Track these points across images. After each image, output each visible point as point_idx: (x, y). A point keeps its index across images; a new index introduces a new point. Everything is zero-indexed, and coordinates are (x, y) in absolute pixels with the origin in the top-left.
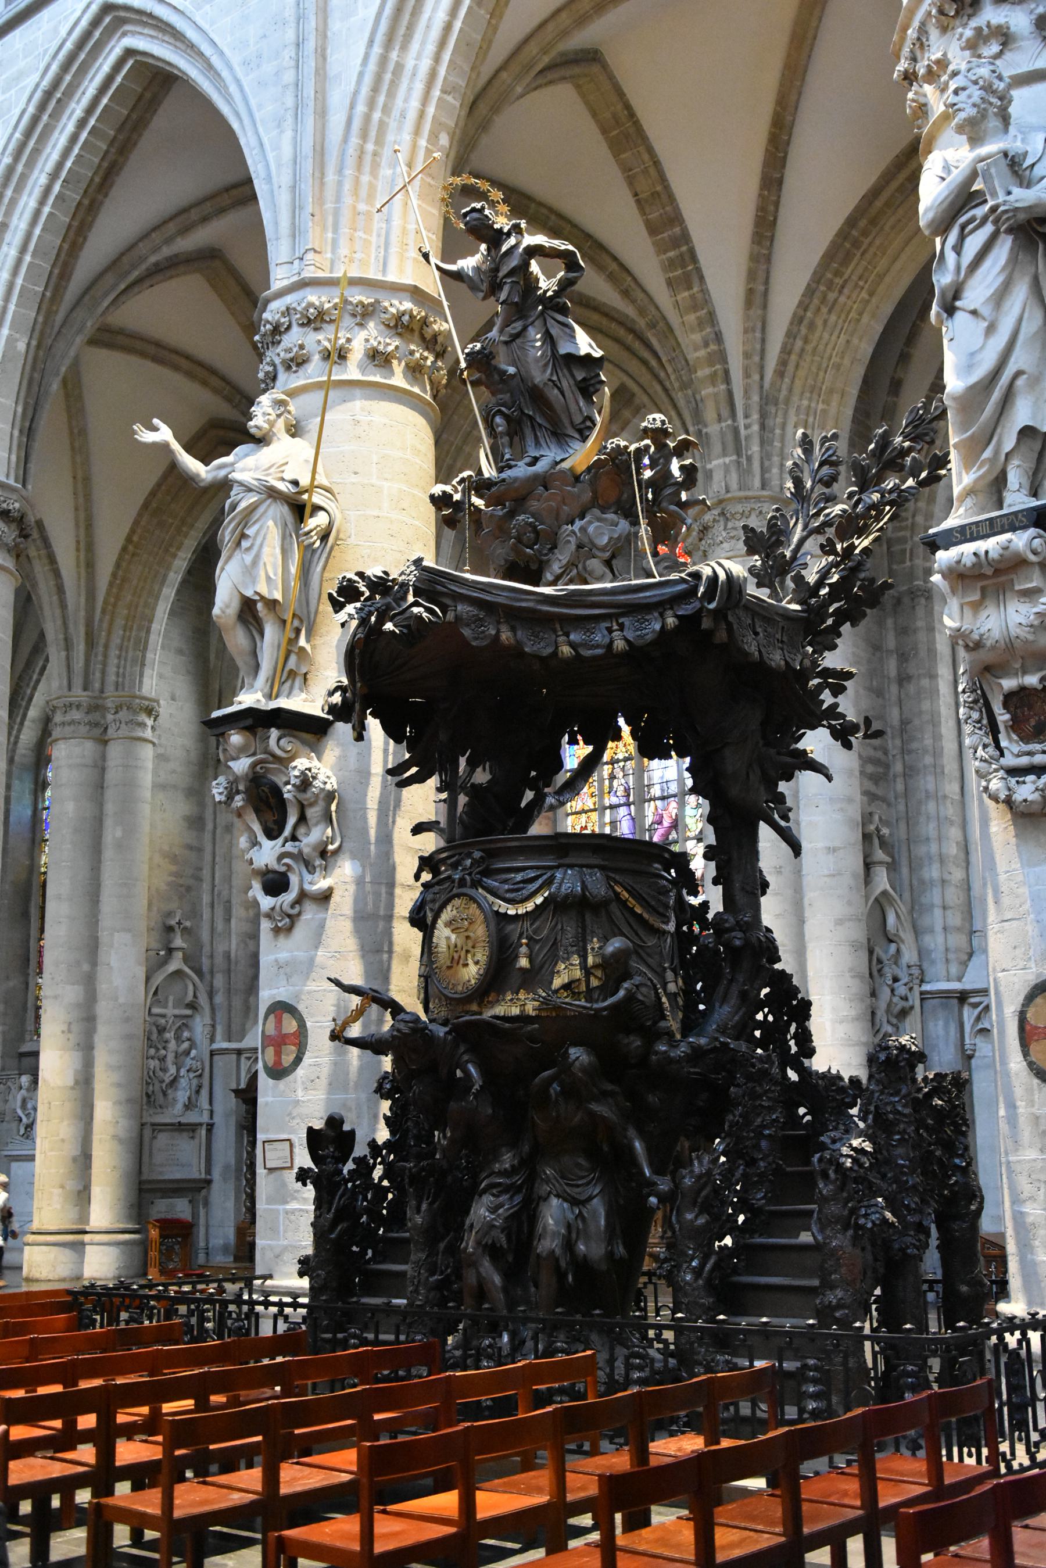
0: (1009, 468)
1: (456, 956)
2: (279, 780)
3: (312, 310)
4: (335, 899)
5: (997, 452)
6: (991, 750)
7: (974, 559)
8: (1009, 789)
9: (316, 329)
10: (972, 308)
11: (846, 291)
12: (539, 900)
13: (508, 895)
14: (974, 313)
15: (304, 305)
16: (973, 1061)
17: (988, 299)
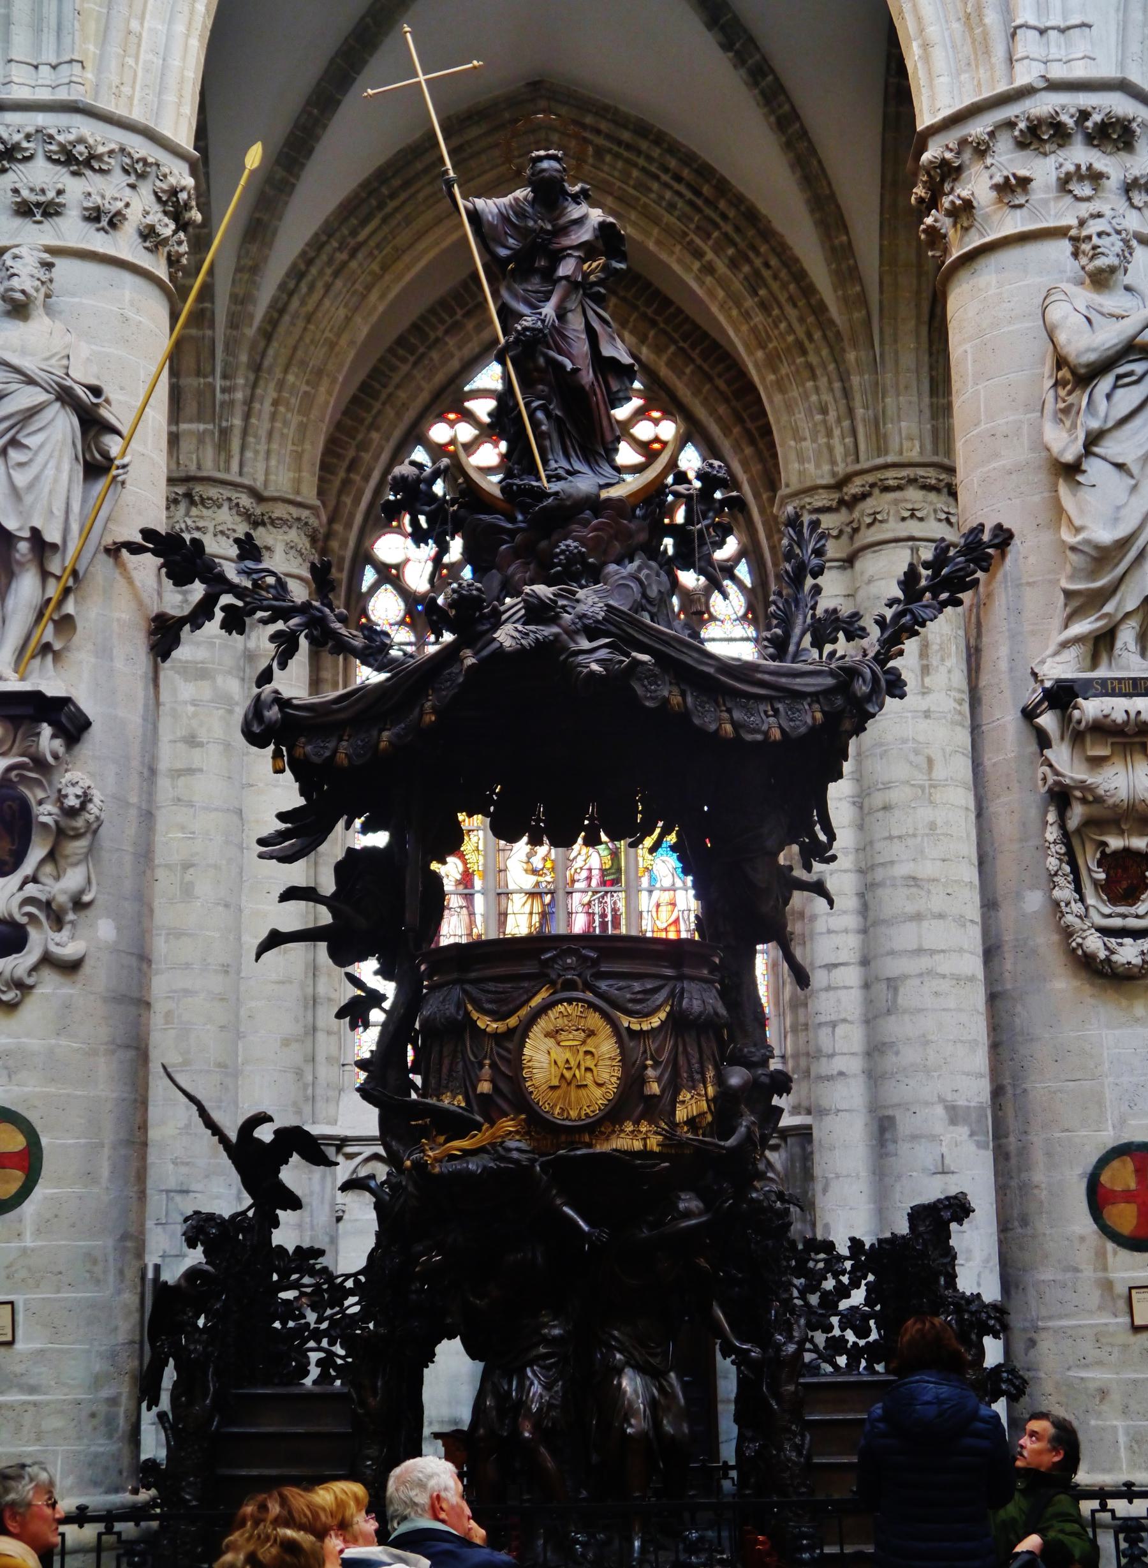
0: (1123, 627)
1: (568, 1075)
2: (32, 795)
4: (86, 969)
5: (1117, 610)
6: (1080, 904)
7: (1125, 717)
8: (1107, 948)
9: (75, 174)
10: (1120, 461)
11: (360, 256)
12: (662, 1015)
14: (1120, 466)
15: (72, 137)
16: (341, 1225)
17: (1139, 459)
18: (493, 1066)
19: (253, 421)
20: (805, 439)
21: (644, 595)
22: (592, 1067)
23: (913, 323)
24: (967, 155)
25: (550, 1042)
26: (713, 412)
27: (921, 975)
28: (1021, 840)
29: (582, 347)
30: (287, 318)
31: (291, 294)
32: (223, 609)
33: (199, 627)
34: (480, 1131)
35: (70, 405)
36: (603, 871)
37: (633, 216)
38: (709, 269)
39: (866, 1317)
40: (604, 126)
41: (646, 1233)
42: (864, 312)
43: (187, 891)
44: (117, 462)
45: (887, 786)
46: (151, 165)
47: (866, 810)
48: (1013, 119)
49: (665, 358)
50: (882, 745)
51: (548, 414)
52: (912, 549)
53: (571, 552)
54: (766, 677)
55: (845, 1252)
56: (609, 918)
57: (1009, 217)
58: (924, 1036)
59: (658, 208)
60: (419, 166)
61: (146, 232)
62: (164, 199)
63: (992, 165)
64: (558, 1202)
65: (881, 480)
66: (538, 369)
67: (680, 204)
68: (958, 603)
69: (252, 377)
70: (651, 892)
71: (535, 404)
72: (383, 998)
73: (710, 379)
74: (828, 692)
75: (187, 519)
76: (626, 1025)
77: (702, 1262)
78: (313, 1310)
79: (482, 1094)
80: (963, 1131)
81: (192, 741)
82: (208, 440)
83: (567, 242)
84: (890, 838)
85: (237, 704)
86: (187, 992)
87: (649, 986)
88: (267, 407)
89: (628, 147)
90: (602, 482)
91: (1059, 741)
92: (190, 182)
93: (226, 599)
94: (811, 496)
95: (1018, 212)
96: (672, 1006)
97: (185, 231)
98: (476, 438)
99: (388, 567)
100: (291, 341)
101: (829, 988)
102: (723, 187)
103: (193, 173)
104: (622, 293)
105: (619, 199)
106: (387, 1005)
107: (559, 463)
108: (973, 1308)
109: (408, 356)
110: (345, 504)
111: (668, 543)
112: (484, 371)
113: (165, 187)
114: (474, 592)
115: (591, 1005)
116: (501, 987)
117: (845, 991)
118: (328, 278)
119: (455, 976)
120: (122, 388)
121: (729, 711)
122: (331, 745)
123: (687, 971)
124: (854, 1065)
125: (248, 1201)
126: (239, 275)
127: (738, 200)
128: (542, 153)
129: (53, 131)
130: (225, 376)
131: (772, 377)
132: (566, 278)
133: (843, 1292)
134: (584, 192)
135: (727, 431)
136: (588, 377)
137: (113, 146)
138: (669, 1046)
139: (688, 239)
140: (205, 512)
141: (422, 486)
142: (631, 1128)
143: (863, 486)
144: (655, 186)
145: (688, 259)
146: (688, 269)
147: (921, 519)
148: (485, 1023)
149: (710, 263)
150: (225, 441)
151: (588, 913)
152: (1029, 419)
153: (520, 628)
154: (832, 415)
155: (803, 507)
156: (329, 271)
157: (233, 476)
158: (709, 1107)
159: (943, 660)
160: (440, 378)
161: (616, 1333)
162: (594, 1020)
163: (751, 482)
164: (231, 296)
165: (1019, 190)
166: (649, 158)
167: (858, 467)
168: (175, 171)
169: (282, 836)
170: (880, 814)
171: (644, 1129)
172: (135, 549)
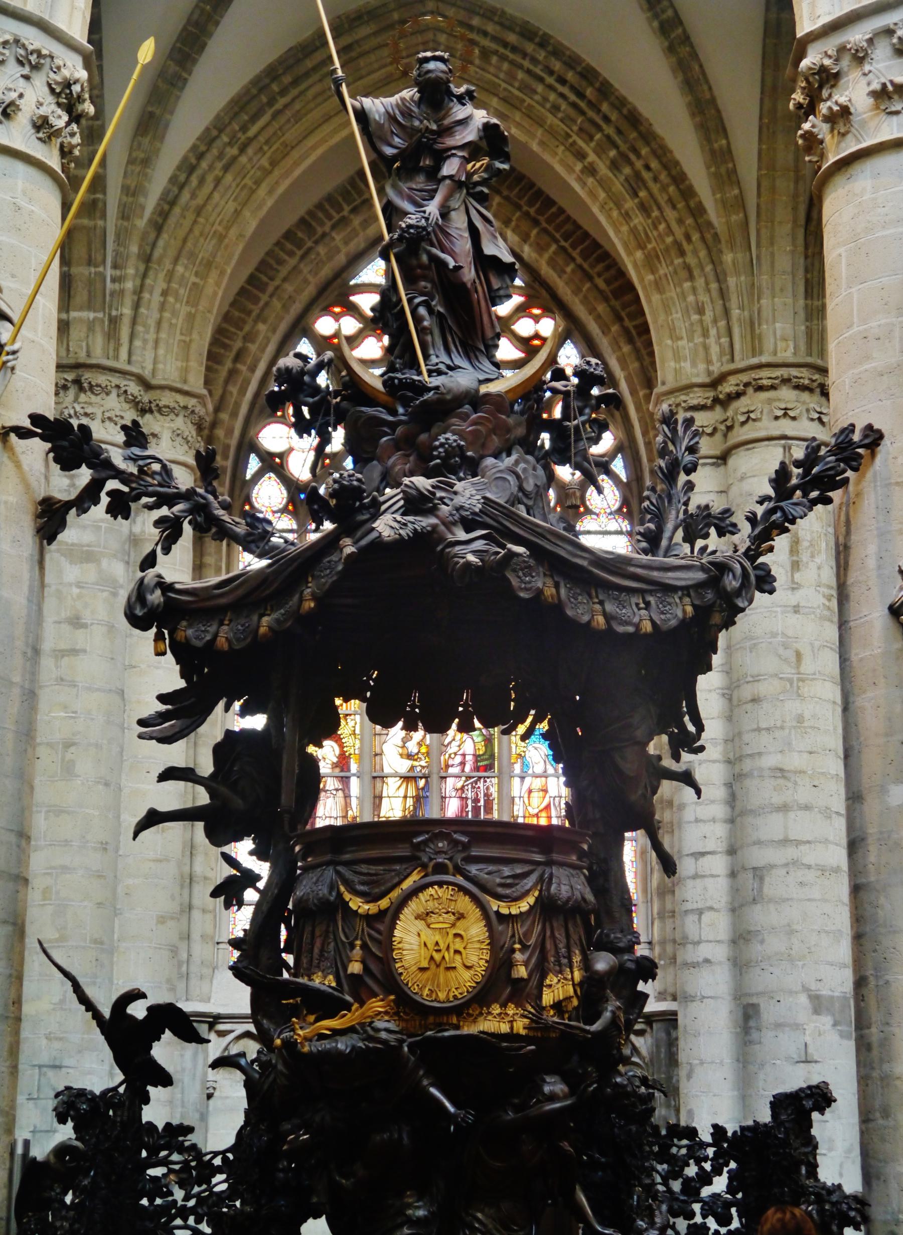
1: (437, 956)
11: (250, 151)
12: (531, 900)
13: (508, 891)
16: (211, 1102)
18: (364, 946)
19: (142, 310)
20: (681, 338)
21: (521, 488)
22: (461, 949)
23: (790, 226)
24: (845, 62)
25: (420, 924)
26: (592, 311)
27: (786, 865)
28: (887, 735)
29: (464, 245)
30: (177, 210)
31: (182, 187)
32: (109, 494)
33: (85, 511)
34: (349, 1010)
36: (476, 757)
37: (518, 116)
38: (591, 170)
39: (728, 1205)
40: (490, 28)
42: (741, 215)
43: (69, 770)
44: (7, 348)
45: (756, 679)
46: (45, 57)
47: (735, 702)
48: (892, 27)
49: (546, 256)
50: (752, 638)
51: (431, 311)
52: (784, 448)
53: (450, 446)
54: (639, 571)
55: (707, 1138)
56: (482, 803)
57: (885, 124)
58: (789, 925)
59: (543, 110)
60: (309, 64)
61: (40, 122)
62: (58, 90)
63: (870, 72)
65: (755, 380)
66: (421, 266)
67: (564, 106)
68: (828, 501)
69: (142, 267)
70: (523, 778)
71: (417, 300)
72: (258, 878)
73: (590, 278)
74: (699, 586)
75: (76, 405)
76: (495, 908)
77: (566, 1146)
78: (180, 1187)
79: (352, 975)
80: (825, 1021)
81: (76, 622)
82: (98, 328)
83: (450, 142)
84: (759, 730)
85: (121, 587)
86: (65, 869)
87: (519, 870)
88: (157, 298)
89: (514, 49)
90: (482, 377)
92: (83, 75)
93: (112, 484)
94: (687, 394)
95: (895, 118)
96: (540, 891)
97: (78, 123)
98: (361, 332)
99: (272, 455)
100: (181, 233)
101: (696, 876)
102: (605, 90)
103: (87, 66)
104: (505, 193)
105: (504, 100)
106: (261, 885)
107: (440, 358)
108: (834, 1198)
109: (295, 249)
110: (231, 393)
111: (545, 438)
112: (369, 267)
113: (58, 78)
114: (355, 483)
115: (461, 888)
116: (373, 869)
117: (711, 880)
118: (218, 172)
119: (328, 857)
120: (13, 276)
121: (601, 603)
122: (213, 629)
123: (555, 857)
124: (719, 953)
125: (120, 1077)
126: (130, 167)
127: (620, 103)
128: (429, 54)
130: (115, 266)
131: (651, 277)
132: (451, 177)
133: (705, 1179)
134: (469, 94)
135: (605, 330)
136: (469, 274)
137: (7, 37)
138: (537, 929)
139: (571, 140)
140: (94, 399)
141: (306, 378)
142: (498, 1011)
143: (737, 385)
144: (540, 88)
145: (571, 159)
146: (570, 169)
147: (794, 418)
148: (356, 904)
149: (591, 164)
150: (115, 329)
151: (461, 798)
153: (399, 518)
154: (708, 316)
155: (678, 405)
156: (219, 165)
157: (122, 364)
158: (575, 991)
159: (812, 556)
160: (326, 272)
161: (479, 1215)
162: (464, 903)
163: (629, 379)
164: (123, 186)
165: (896, 97)
166: (534, 60)
167: (732, 367)
168: (69, 64)
169: (163, 717)
170: (749, 707)
171: (511, 1012)
172: (23, 433)
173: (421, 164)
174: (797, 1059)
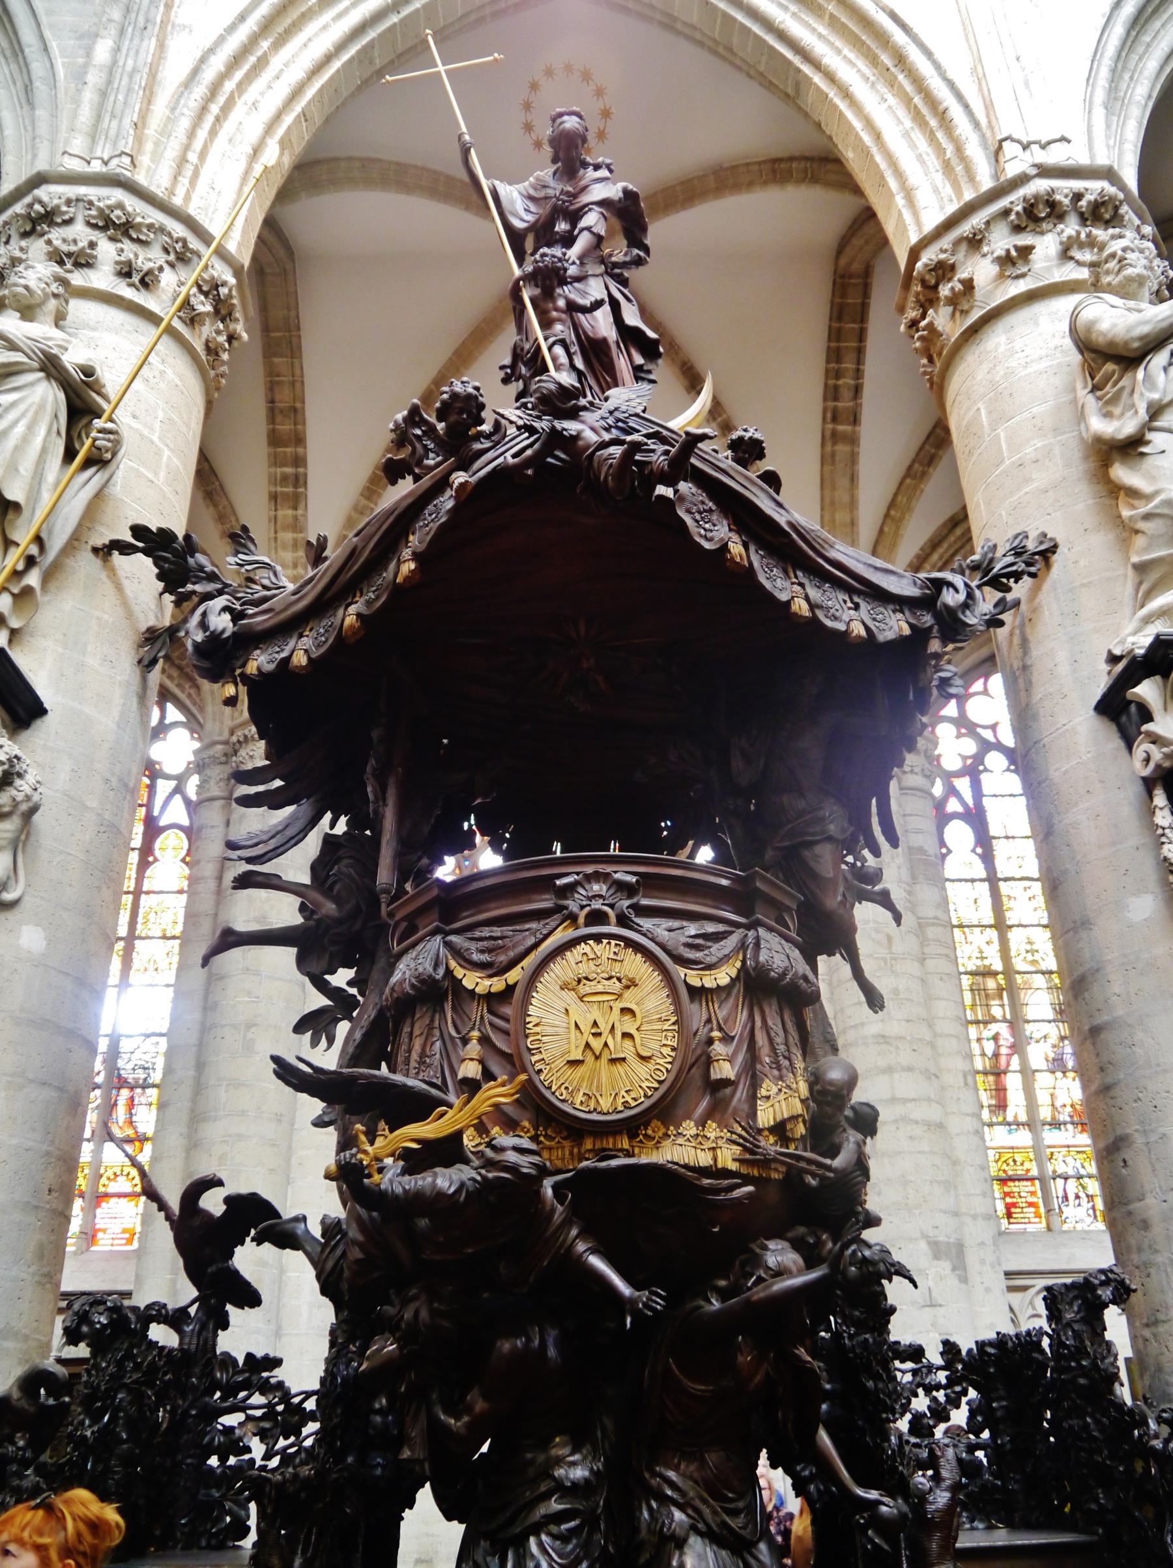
1: (597, 1044)
3: (118, 212)
9: (112, 239)
18: (484, 1040)
22: (633, 1031)
25: (570, 996)
27: (896, 1121)
35: (56, 379)
41: (716, 1304)
55: (938, 1360)
58: (903, 1176)
64: (581, 1247)
80: (945, 1266)
83: (586, 199)
86: (240, 1137)
87: (711, 928)
91: (1162, 711)
96: (744, 962)
116: (497, 931)
120: (134, 417)
121: (801, 585)
129: (94, 199)
133: (939, 1413)
137: (149, 221)
138: (742, 1016)
142: (694, 1131)
148: (472, 980)
152: (1059, 441)
159: (893, 858)
161: (671, 1474)
165: (1020, 262)
171: (712, 1135)
173: (557, 229)
174: (923, 1303)
